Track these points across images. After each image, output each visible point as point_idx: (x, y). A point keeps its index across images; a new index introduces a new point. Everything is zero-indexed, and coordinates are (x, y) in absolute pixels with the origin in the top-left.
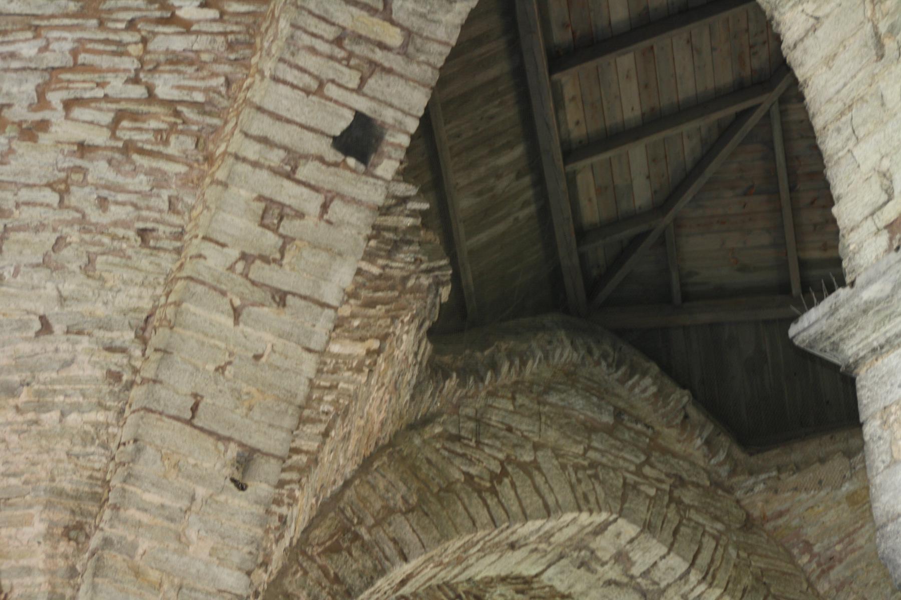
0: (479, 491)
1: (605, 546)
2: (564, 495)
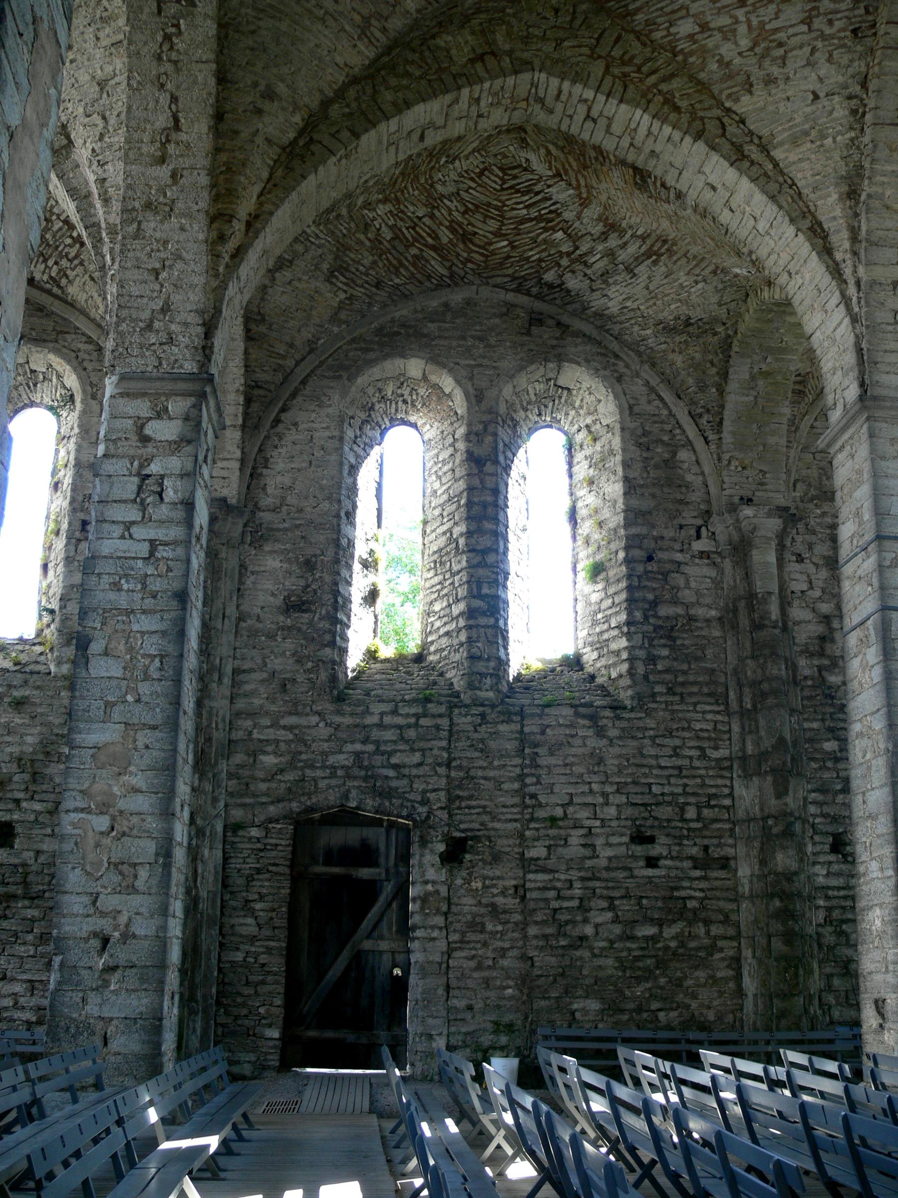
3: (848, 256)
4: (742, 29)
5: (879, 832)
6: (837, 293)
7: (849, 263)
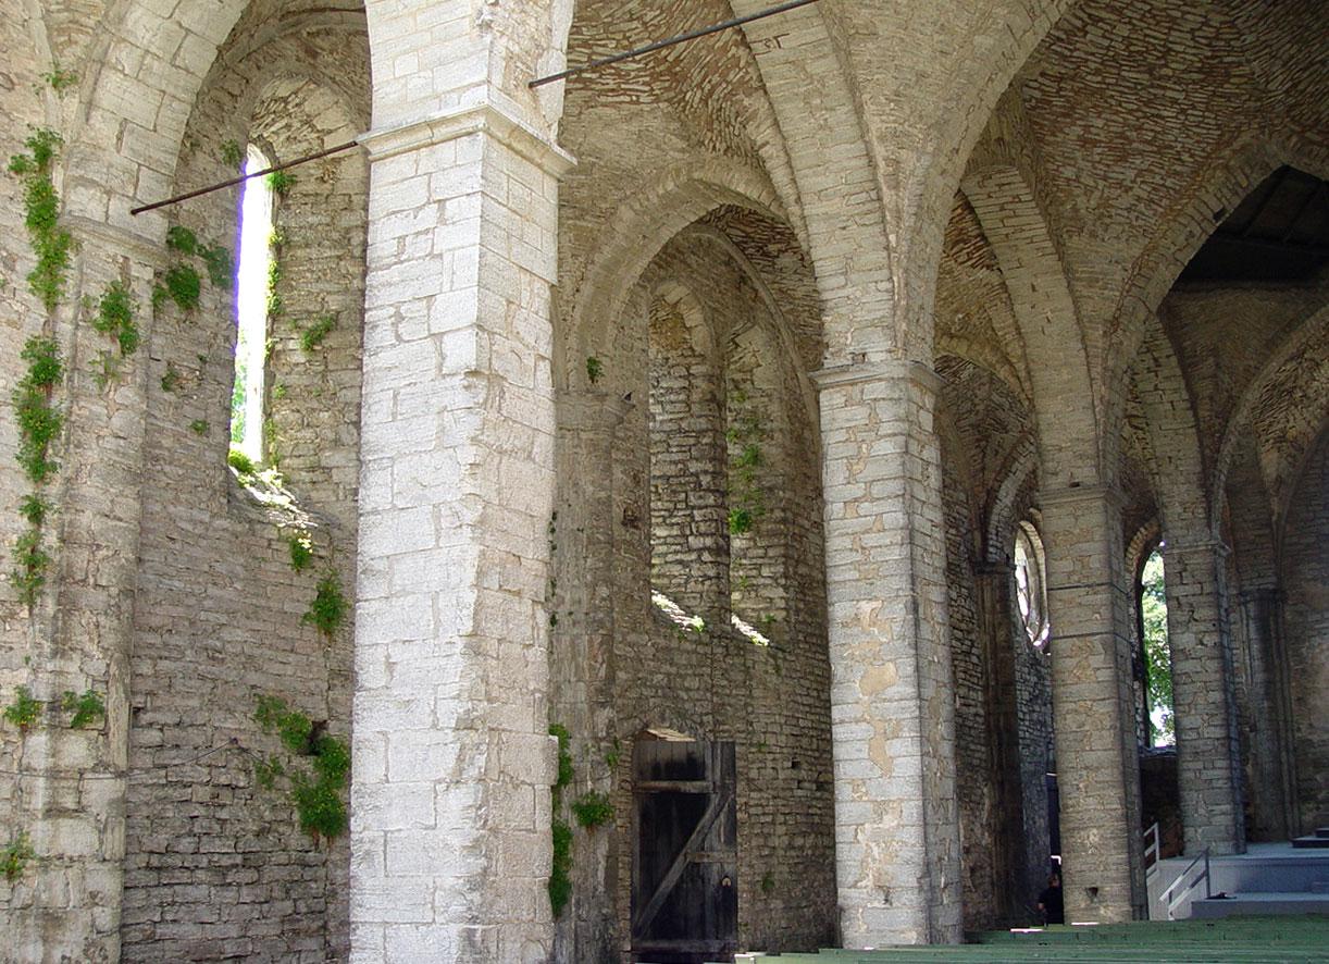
4: (1097, 194)
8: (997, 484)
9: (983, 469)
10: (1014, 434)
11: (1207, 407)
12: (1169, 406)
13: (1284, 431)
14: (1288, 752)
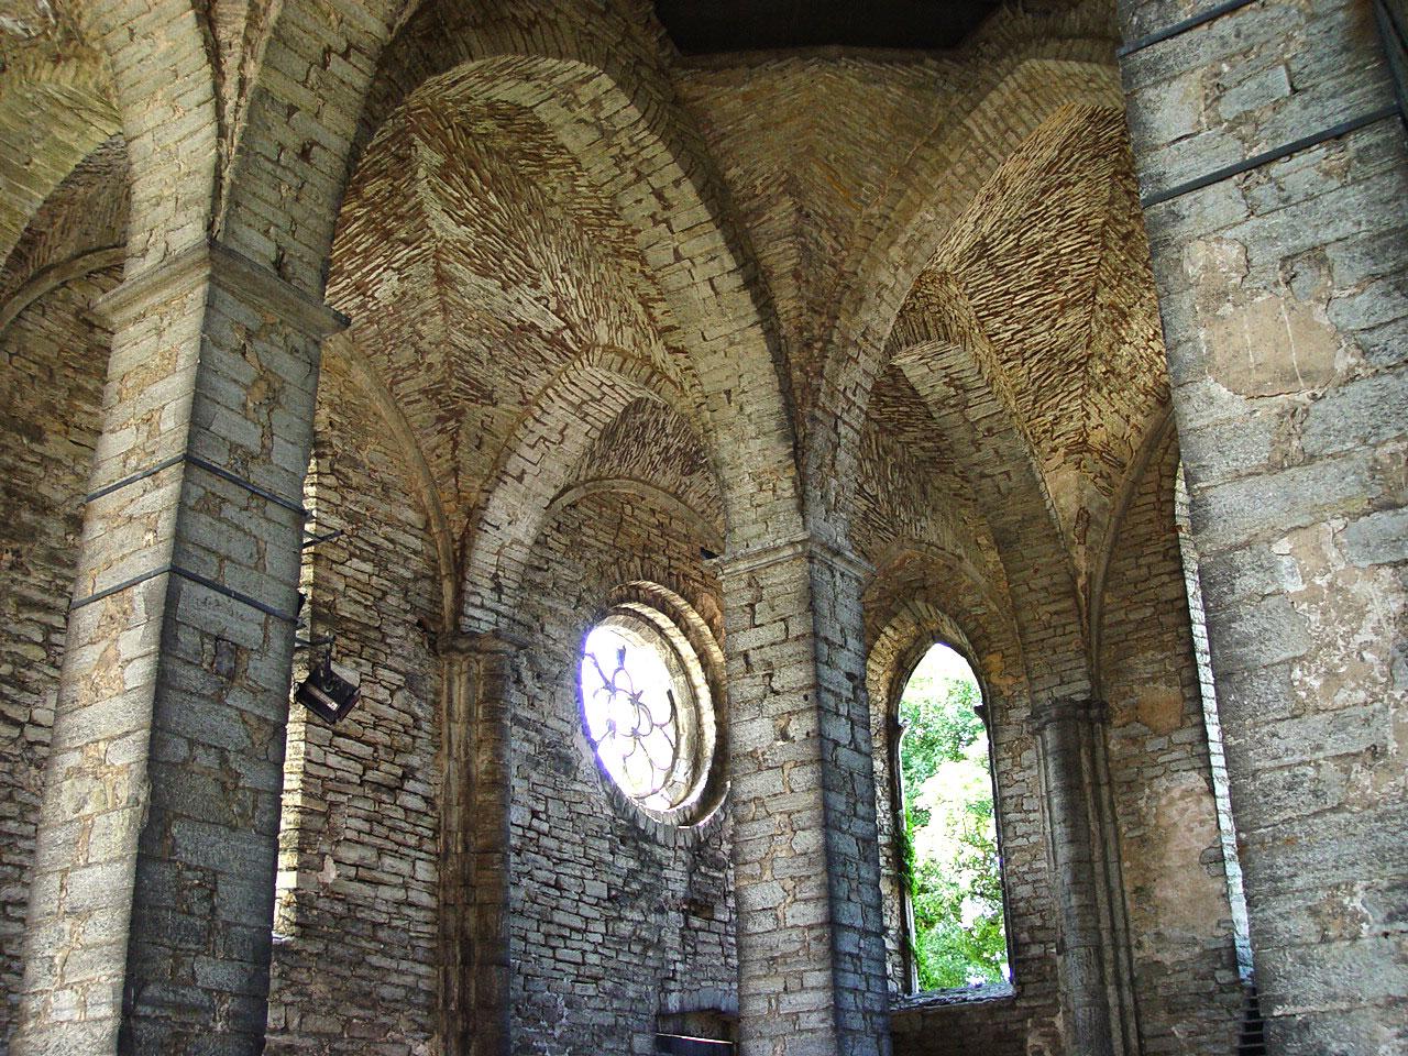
0: (520, 27)
1: (586, 93)
2: (573, 49)
3: (238, 41)
5: (89, 940)
6: (208, 85)
7: (237, 51)
8: (483, 497)
9: (455, 471)
10: (509, 406)
11: (791, 292)
12: (707, 291)
13: (1083, 432)
14: (1119, 986)
